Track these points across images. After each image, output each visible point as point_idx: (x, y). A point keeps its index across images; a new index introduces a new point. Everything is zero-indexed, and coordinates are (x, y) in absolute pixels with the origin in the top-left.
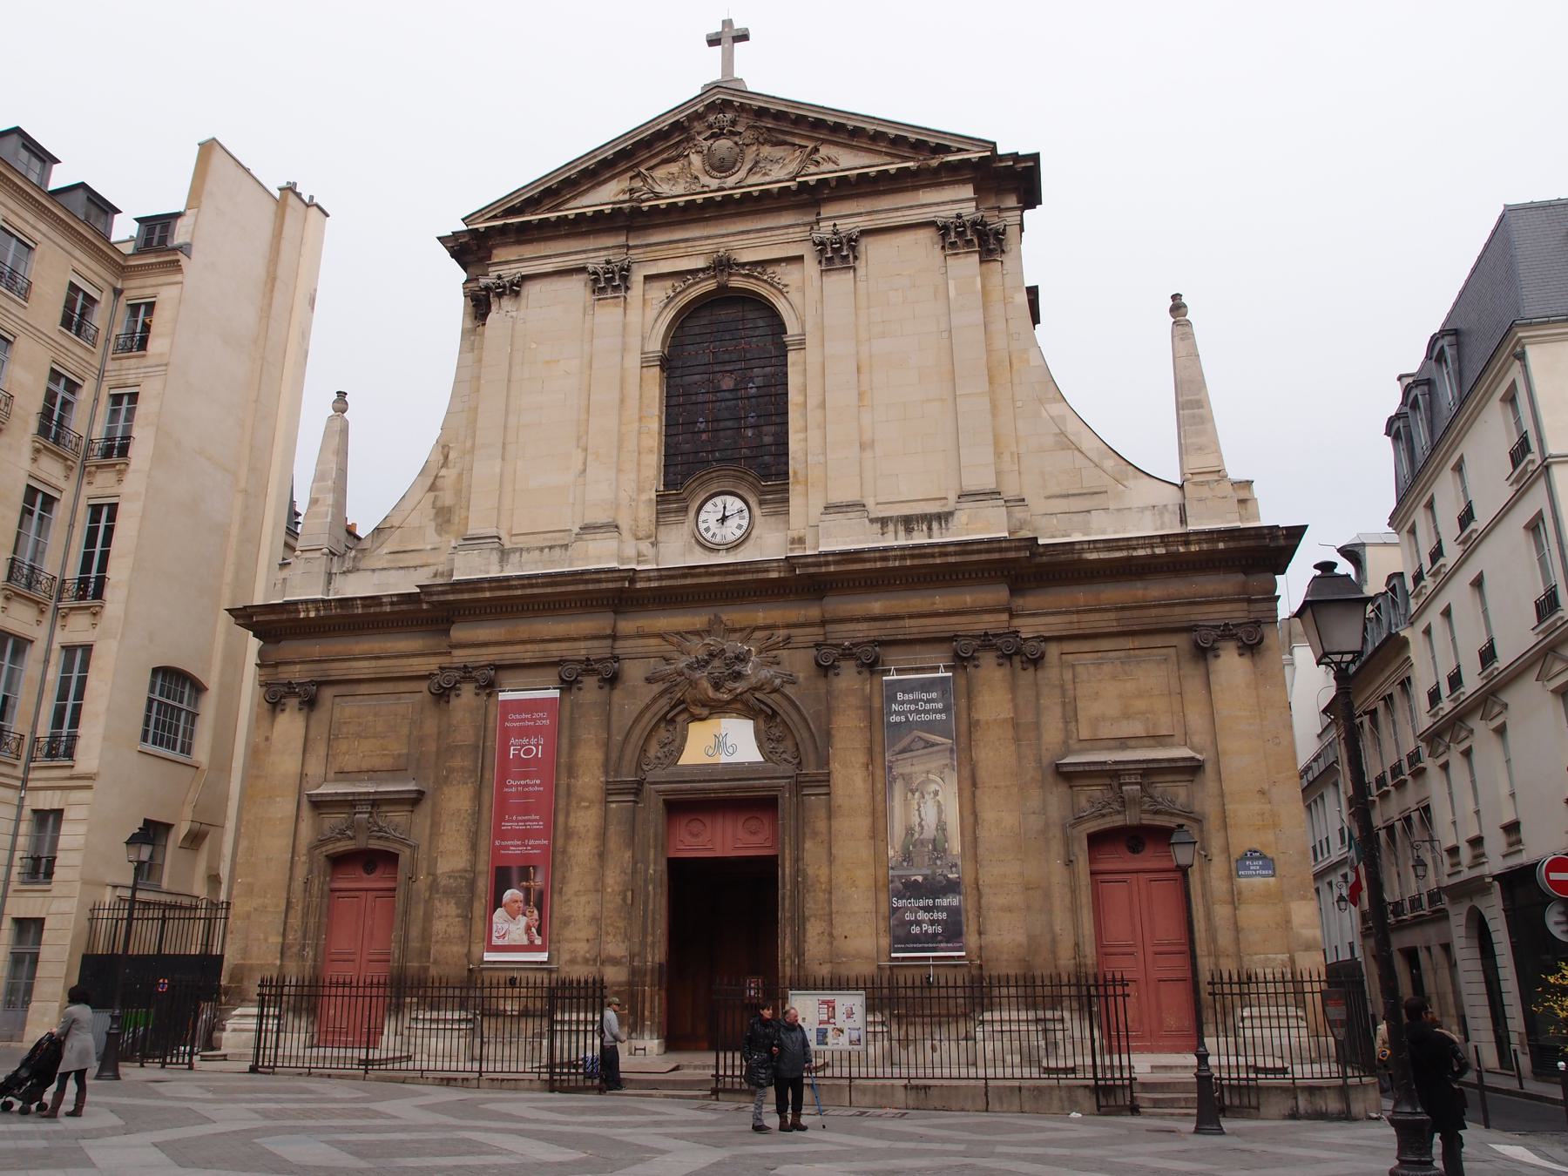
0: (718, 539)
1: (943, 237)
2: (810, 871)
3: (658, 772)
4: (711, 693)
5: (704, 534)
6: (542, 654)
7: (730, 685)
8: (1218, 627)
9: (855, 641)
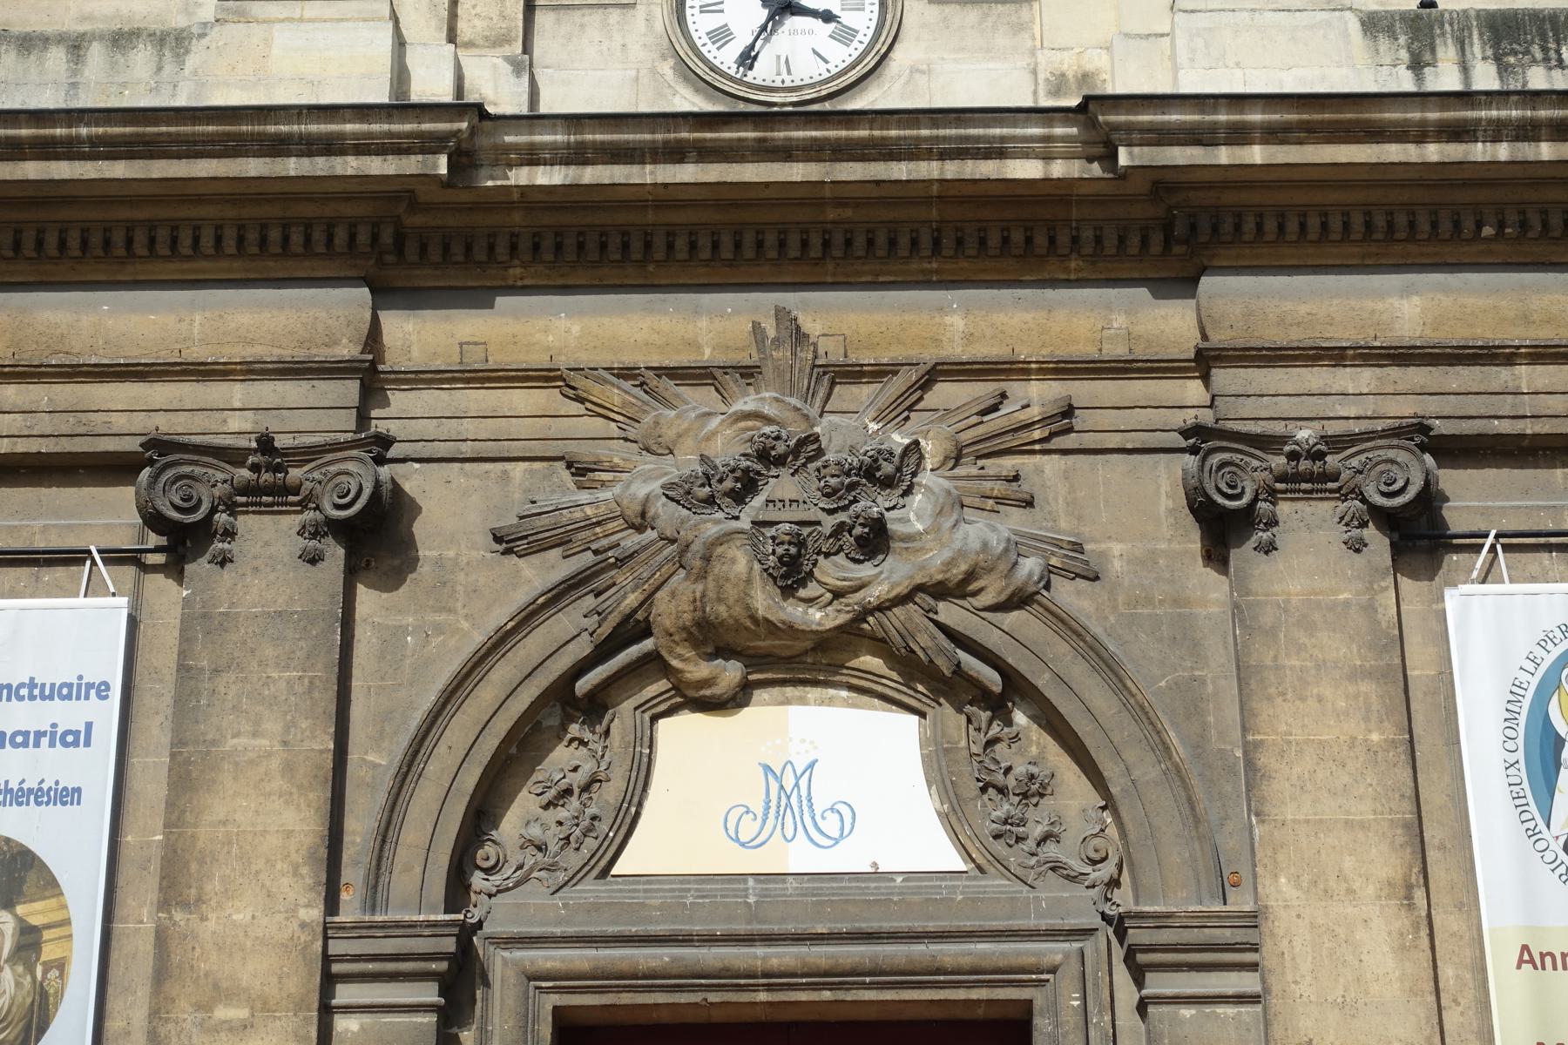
3: (535, 895)
4: (764, 600)
5: (710, 51)
6: (66, 424)
7: (833, 570)
9: (1334, 428)
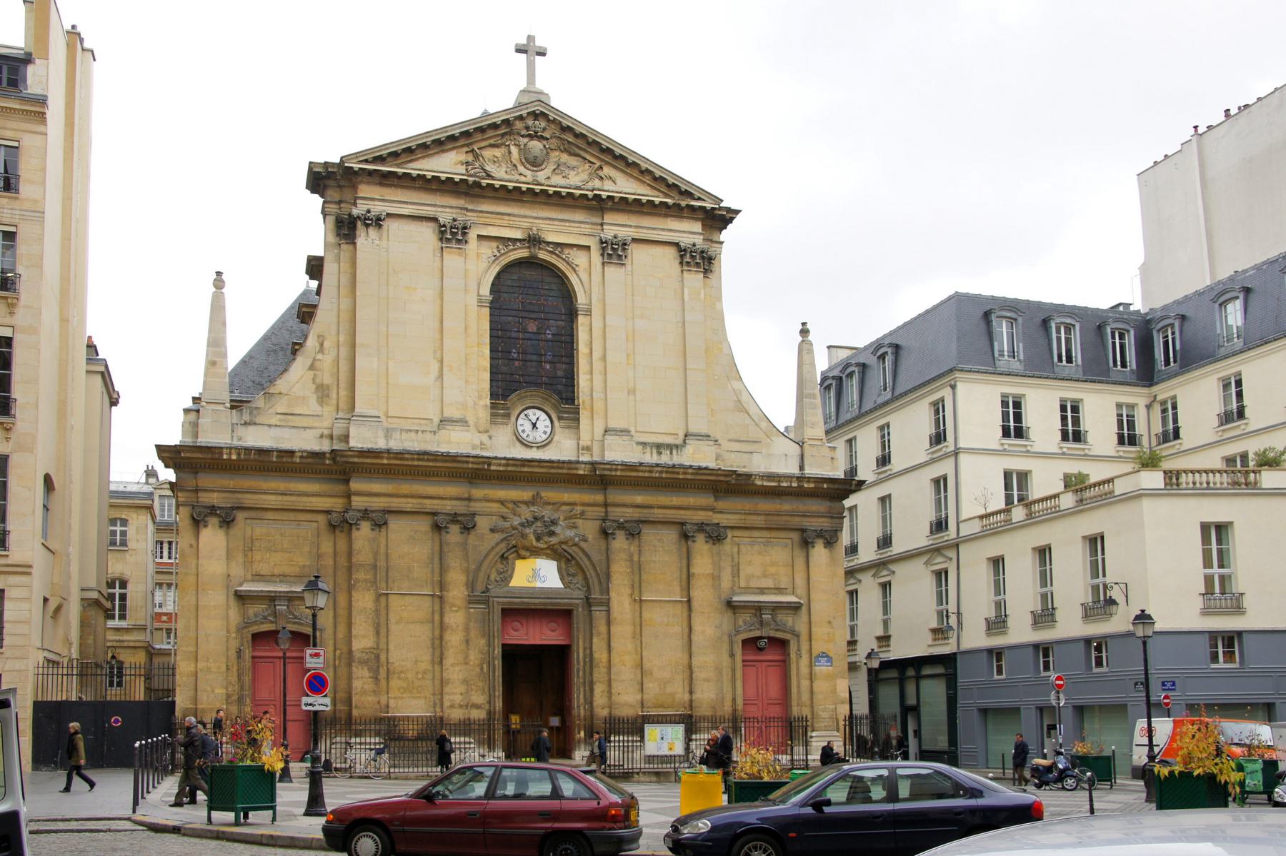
0: (530, 439)
1: (682, 257)
2: (596, 655)
4: (534, 543)
5: (521, 434)
6: (419, 506)
7: (546, 538)
8: (816, 531)
9: (627, 519)
